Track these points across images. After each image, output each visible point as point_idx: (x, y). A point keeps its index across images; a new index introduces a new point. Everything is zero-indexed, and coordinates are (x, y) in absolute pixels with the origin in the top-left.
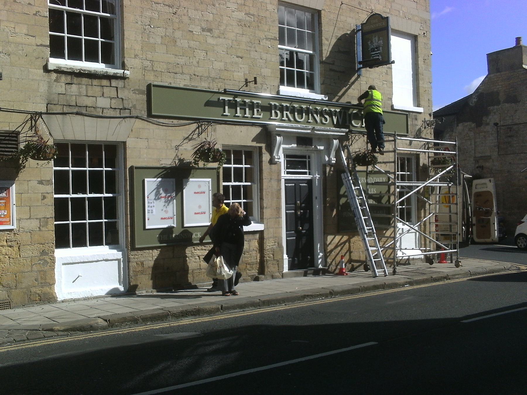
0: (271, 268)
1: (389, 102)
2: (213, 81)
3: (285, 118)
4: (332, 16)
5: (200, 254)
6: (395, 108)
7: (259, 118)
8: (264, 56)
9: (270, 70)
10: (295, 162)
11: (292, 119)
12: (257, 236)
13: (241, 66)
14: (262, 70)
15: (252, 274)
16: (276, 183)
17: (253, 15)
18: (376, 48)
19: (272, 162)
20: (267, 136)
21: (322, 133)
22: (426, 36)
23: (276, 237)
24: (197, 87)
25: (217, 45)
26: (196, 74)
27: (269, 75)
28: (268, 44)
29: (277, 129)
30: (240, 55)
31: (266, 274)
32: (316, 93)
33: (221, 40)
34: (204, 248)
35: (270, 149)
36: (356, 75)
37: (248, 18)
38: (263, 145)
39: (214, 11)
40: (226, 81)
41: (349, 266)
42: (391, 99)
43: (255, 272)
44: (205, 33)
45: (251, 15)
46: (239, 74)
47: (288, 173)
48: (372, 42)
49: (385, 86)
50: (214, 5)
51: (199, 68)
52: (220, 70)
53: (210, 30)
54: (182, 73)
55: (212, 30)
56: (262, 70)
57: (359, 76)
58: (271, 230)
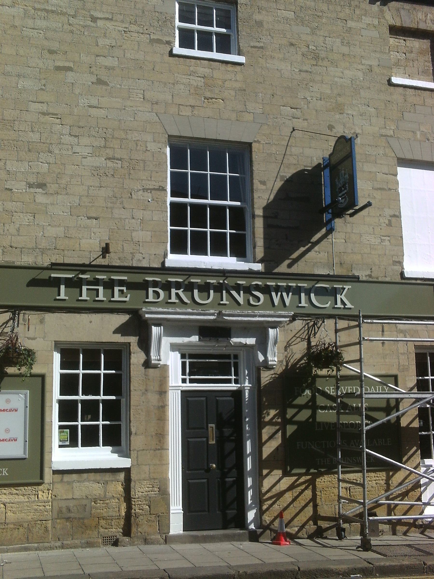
0: (144, 525)
1: (397, 268)
2: (43, 253)
3: (174, 299)
4: (273, 149)
5: (8, 501)
6: (406, 276)
7: (125, 302)
8: (139, 214)
9: (149, 233)
10: (197, 365)
11: (186, 300)
12: (122, 476)
13: (95, 230)
14: (134, 234)
15: (110, 534)
16: (157, 396)
17: (120, 160)
18: (343, 186)
19: (147, 364)
20: (139, 327)
21: (240, 319)
23: (154, 479)
24: (14, 262)
25: (52, 204)
26: (13, 244)
27: (148, 239)
28: (148, 196)
29: (147, 316)
30: (94, 215)
31: (132, 535)
32: (246, 262)
33: (60, 197)
34: (15, 491)
35: (145, 345)
36: (324, 231)
37: (110, 164)
38: (133, 340)
39: (52, 160)
40: (66, 252)
41: (311, 527)
42: (400, 263)
43: (116, 530)
44: (32, 190)
45: (117, 159)
46: (91, 241)
47: (191, 381)
48: (339, 179)
49: (387, 243)
50: (51, 152)
51: (19, 238)
52: (56, 238)
53: (42, 185)
55: (45, 185)
56: (134, 234)
57: (330, 231)
58: (146, 468)
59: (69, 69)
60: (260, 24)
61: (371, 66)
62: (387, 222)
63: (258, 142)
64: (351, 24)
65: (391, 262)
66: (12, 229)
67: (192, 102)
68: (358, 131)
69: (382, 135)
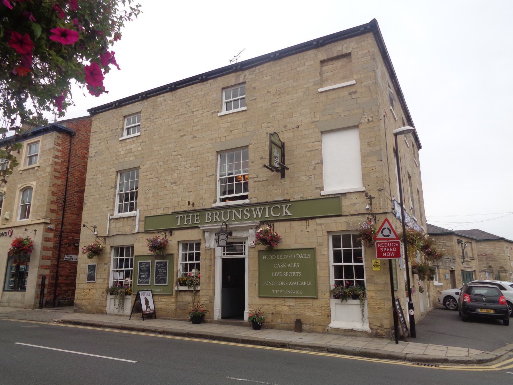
17: (199, 166)
22: (372, 121)
28: (208, 179)
37: (196, 169)
39: (178, 172)
47: (227, 254)
49: (313, 179)
53: (175, 183)
54: (160, 208)
59: (184, 135)
60: (254, 88)
61: (308, 87)
62: (313, 167)
63: (251, 144)
64: (298, 69)
65: (314, 188)
66: (166, 200)
67: (225, 135)
68: (300, 124)
69: (313, 122)
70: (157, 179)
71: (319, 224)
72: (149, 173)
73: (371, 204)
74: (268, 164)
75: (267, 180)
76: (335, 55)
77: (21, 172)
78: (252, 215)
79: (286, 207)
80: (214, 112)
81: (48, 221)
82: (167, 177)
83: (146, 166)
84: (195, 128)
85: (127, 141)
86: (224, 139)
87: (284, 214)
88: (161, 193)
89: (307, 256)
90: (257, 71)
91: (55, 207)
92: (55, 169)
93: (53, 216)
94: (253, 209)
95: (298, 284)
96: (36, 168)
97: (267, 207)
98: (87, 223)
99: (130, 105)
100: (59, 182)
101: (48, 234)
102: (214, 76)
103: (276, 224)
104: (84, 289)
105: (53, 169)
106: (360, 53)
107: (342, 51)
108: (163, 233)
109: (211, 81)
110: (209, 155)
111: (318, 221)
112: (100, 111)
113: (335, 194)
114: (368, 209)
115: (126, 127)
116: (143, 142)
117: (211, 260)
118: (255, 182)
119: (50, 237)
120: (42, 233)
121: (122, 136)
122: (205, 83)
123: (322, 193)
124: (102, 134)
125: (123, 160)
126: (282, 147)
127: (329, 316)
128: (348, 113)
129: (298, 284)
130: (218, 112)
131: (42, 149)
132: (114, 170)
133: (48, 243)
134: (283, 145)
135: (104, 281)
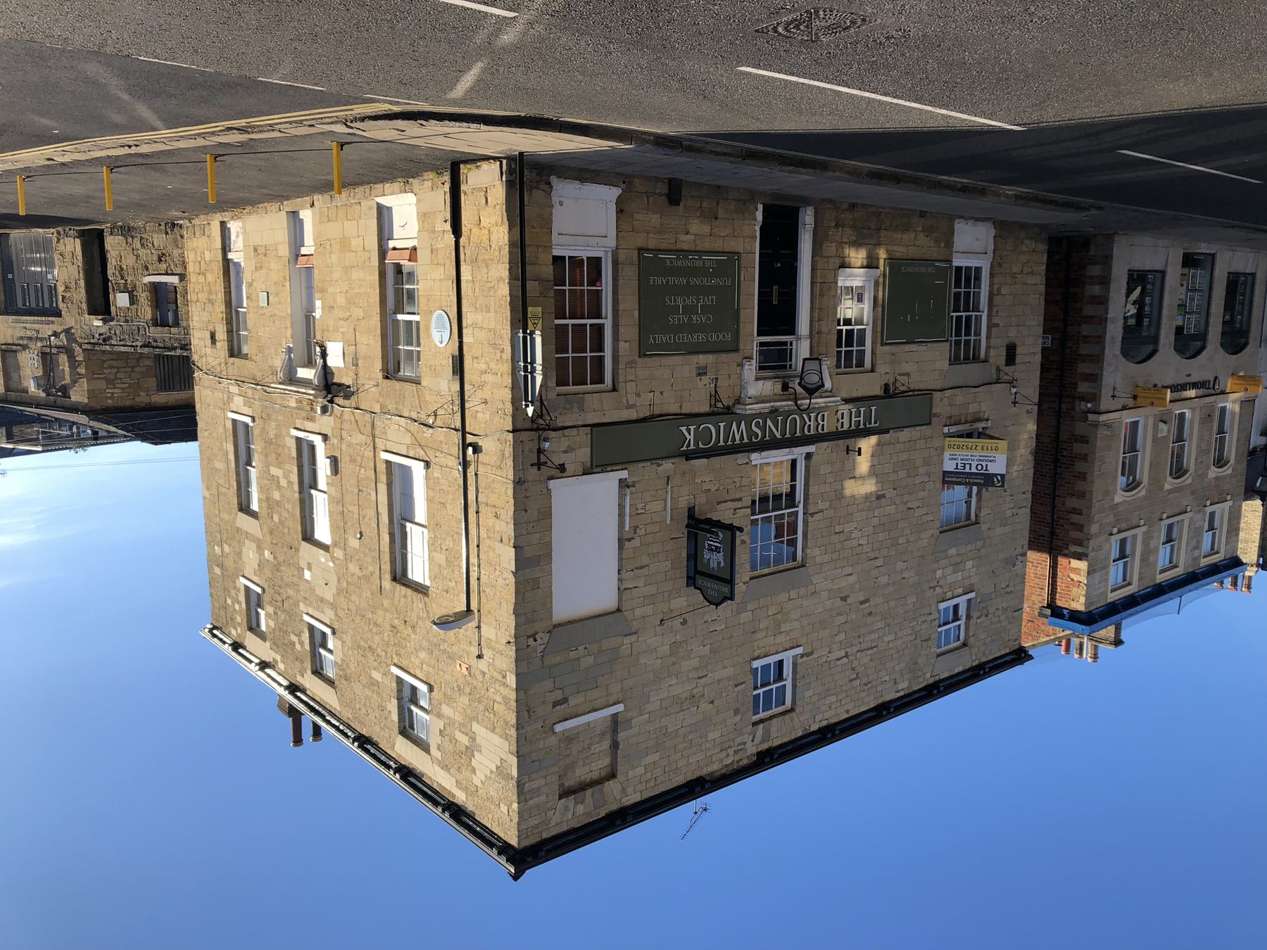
22: (529, 637)
28: (821, 506)
59: (862, 603)
60: (737, 712)
64: (656, 757)
68: (658, 628)
70: (909, 505)
71: (632, 406)
72: (925, 518)
73: (540, 451)
74: (738, 533)
75: (719, 503)
76: (589, 792)
77: (1142, 522)
78: (749, 427)
79: (689, 445)
80: (808, 655)
81: (1091, 417)
82: (891, 509)
83: (929, 534)
84: (842, 619)
85: (960, 591)
86: (793, 594)
87: (692, 428)
88: (902, 474)
89: (654, 339)
90: (731, 751)
91: (1078, 448)
92: (1081, 531)
93: (1080, 428)
94: (746, 440)
95: (673, 280)
96: (1115, 530)
97: (722, 443)
98: (1028, 412)
99: (956, 671)
100: (1071, 503)
101: (1090, 390)
102: (811, 738)
103: (705, 408)
104: (1032, 273)
105: (1085, 530)
106: (543, 798)
107: (576, 803)
108: (904, 388)
109: (814, 727)
110: (818, 560)
111: (632, 415)
112: (1008, 658)
113: (603, 472)
114: (546, 440)
115: (962, 622)
116: (934, 588)
117: (819, 333)
118: (740, 499)
119: (1086, 384)
120: (1103, 392)
121: (969, 601)
122: (825, 723)
123: (624, 474)
124: (1005, 605)
125: (969, 547)
126: (696, 574)
127: (620, 211)
128: (572, 655)
129: (673, 280)
130: (802, 656)
131: (1107, 574)
132: (984, 527)
133: (1088, 371)
134: (691, 581)
135: (999, 289)
